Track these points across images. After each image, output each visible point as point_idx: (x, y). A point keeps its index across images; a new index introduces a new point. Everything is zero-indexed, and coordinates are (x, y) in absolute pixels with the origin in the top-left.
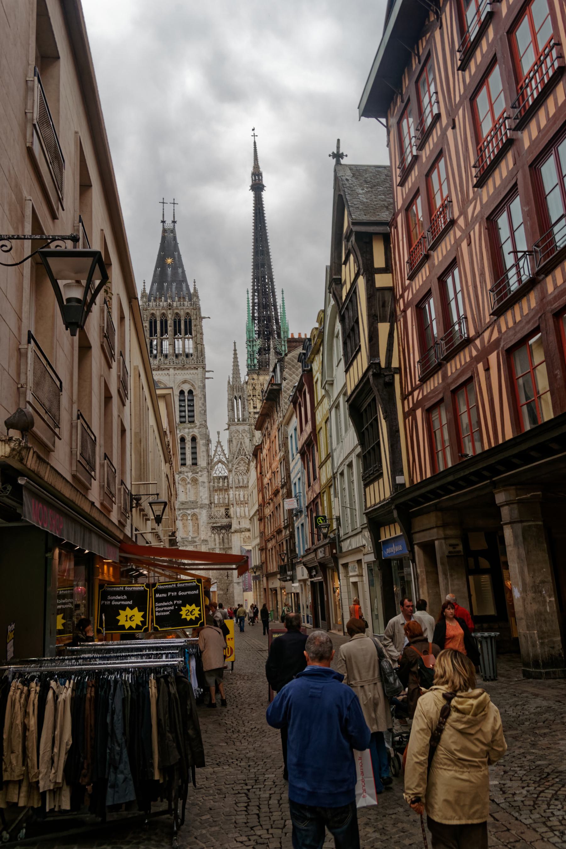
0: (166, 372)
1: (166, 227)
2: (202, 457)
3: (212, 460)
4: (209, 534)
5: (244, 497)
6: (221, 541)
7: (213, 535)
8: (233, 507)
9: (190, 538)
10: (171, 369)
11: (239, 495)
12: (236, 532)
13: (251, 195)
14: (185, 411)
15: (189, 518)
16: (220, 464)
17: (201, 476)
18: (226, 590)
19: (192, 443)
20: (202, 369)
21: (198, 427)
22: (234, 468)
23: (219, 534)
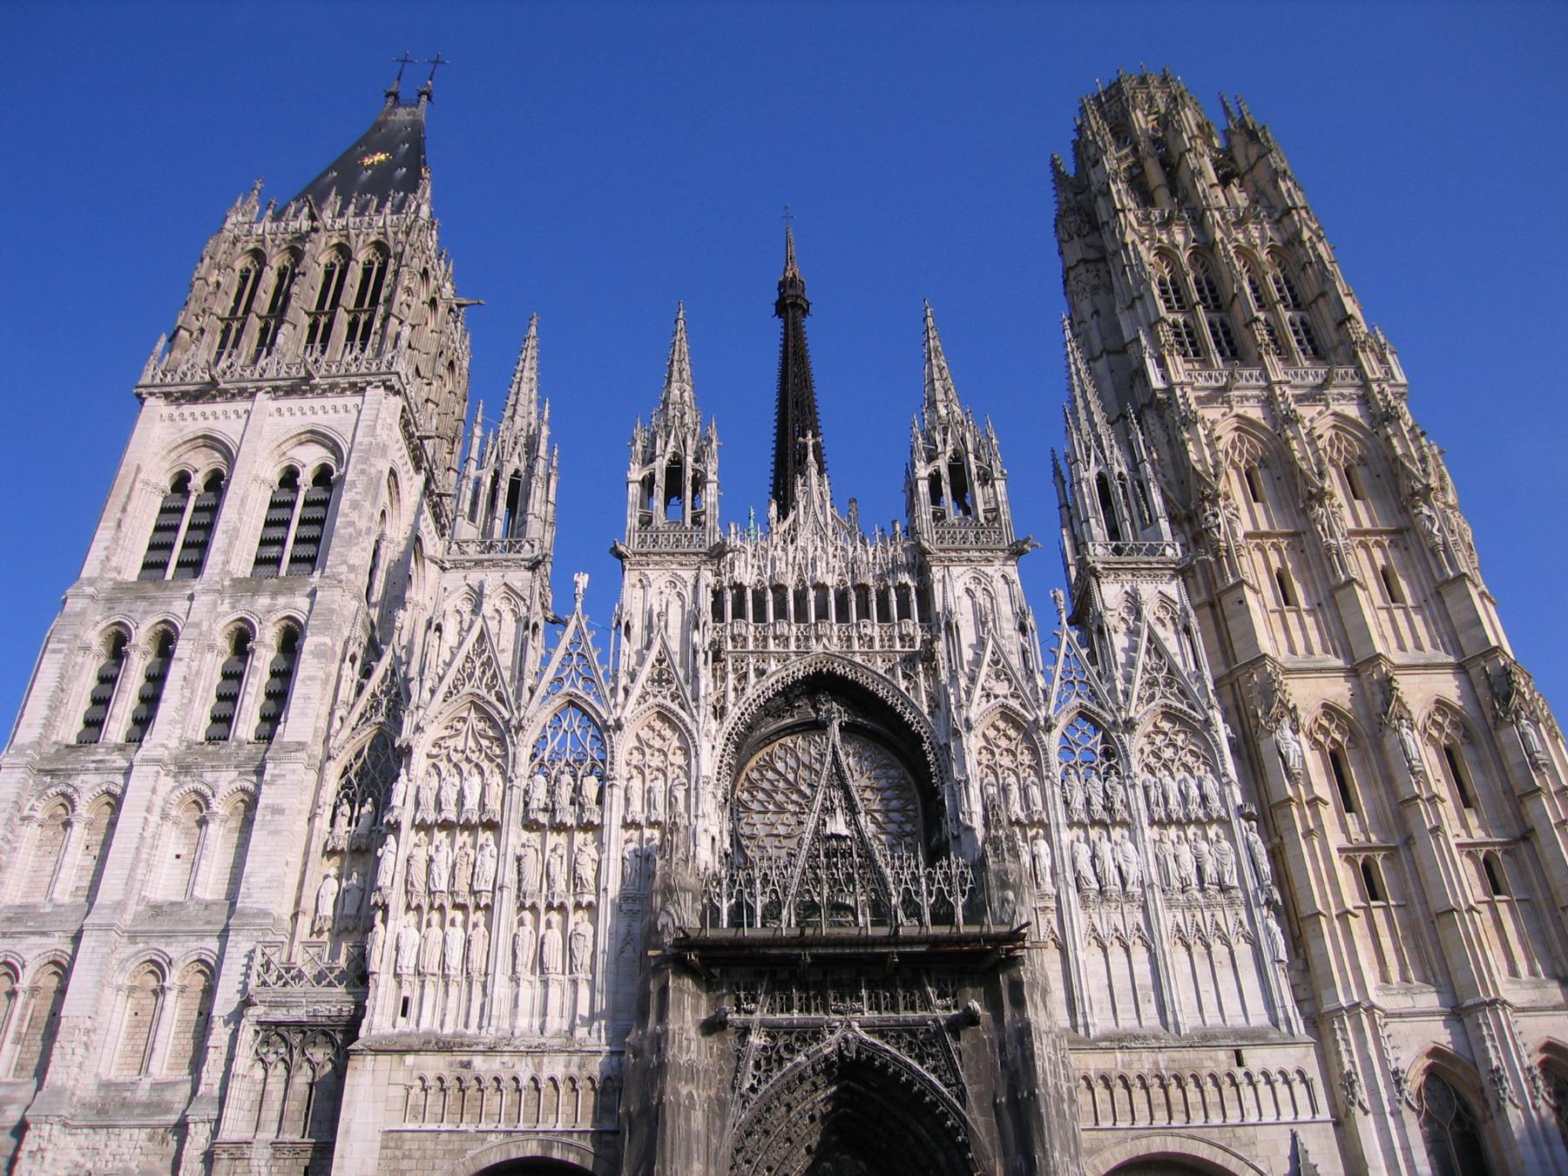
0: (241, 405)
6: (296, 1105)
8: (385, 921)
9: (146, 1083)
10: (260, 395)
14: (282, 542)
17: (272, 782)
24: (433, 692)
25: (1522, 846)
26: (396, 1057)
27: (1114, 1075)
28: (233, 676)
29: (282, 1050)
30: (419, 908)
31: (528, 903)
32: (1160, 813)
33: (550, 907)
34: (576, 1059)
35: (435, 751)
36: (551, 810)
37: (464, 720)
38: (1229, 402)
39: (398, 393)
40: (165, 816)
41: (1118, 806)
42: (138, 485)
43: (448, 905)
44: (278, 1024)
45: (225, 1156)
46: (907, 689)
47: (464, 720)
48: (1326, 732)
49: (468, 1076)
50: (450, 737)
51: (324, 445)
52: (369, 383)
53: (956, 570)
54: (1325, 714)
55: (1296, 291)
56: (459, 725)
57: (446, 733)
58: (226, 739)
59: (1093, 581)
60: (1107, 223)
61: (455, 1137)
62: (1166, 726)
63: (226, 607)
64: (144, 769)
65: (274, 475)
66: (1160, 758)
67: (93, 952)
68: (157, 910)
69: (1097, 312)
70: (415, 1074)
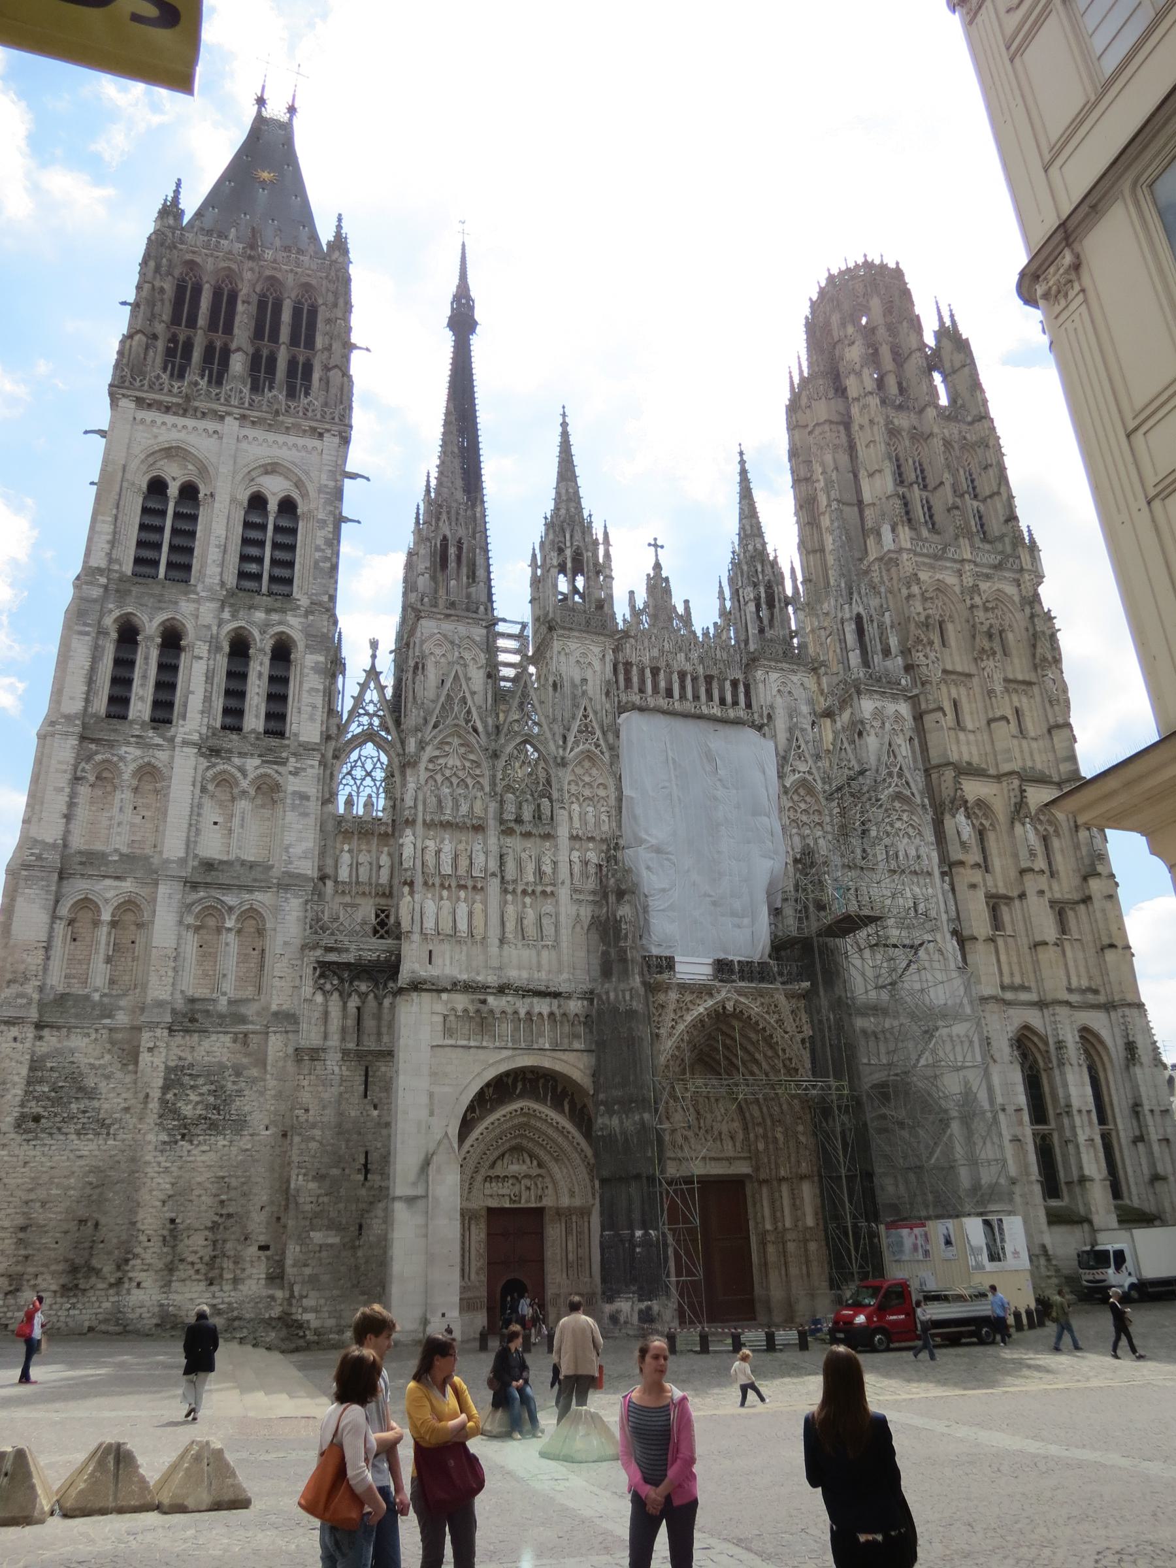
0: (211, 425)
1: (264, 114)
2: (306, 710)
3: (342, 728)
4: (307, 989)
5: (455, 866)
6: (351, 1022)
7: (319, 998)
8: (412, 893)
9: (223, 1001)
10: (228, 419)
11: (438, 852)
12: (416, 986)
13: (447, 340)
14: (260, 560)
15: (229, 924)
16: (370, 745)
17: (295, 773)
18: (353, 1229)
19: (271, 665)
20: (337, 440)
21: (302, 611)
22: (425, 756)
23: (344, 997)
24: (426, 721)
25: (1082, 907)
26: (434, 994)
27: (869, 1031)
28: (237, 676)
29: (335, 982)
30: (433, 884)
32: (893, 865)
33: (524, 892)
34: (555, 1002)
35: (431, 766)
36: (519, 820)
37: (448, 743)
40: (204, 790)
41: (870, 857)
42: (125, 484)
43: (454, 884)
45: (306, 1058)
47: (448, 743)
48: (977, 817)
49: (484, 1008)
51: (287, 478)
53: (774, 676)
54: (978, 805)
55: (976, 483)
56: (447, 748)
57: (437, 753)
58: (238, 729)
59: (855, 696)
60: (857, 399)
61: (480, 1051)
62: (897, 805)
63: (226, 615)
64: (185, 749)
65: (244, 496)
66: (892, 826)
67: (170, 898)
68: (209, 866)
69: (837, 469)
70: (449, 1006)
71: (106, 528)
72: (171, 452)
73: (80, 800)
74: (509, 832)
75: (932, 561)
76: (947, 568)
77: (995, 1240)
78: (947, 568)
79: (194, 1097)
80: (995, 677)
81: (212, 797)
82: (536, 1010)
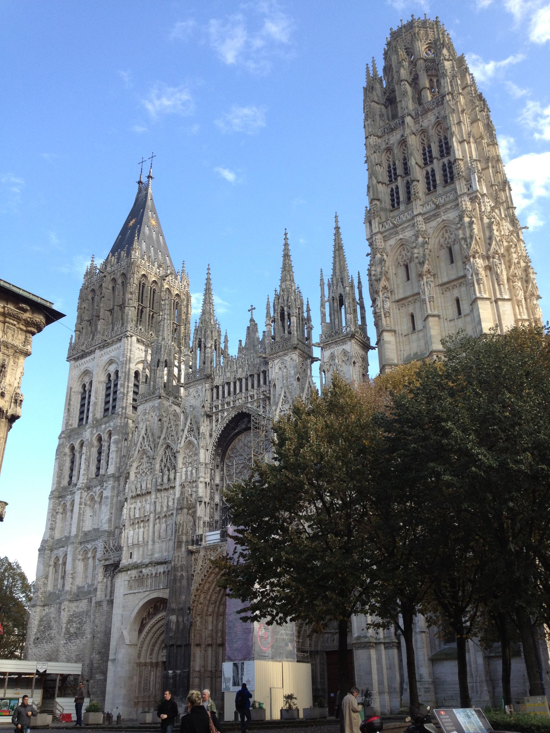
10: (96, 350)
11: (135, 508)
28: (100, 453)
31: (157, 517)
34: (166, 566)
37: (143, 458)
38: (398, 233)
39: (131, 336)
40: (85, 505)
42: (72, 394)
44: (107, 565)
46: (264, 412)
50: (141, 465)
52: (122, 337)
53: (276, 362)
56: (143, 461)
61: (139, 594)
63: (95, 431)
65: (104, 378)
68: (86, 534)
71: (66, 415)
72: (86, 372)
73: (58, 521)
74: (159, 490)
75: (395, 230)
76: (406, 228)
77: (238, 674)
78: (406, 228)
79: (75, 626)
80: (426, 290)
81: (90, 506)
82: (159, 572)
